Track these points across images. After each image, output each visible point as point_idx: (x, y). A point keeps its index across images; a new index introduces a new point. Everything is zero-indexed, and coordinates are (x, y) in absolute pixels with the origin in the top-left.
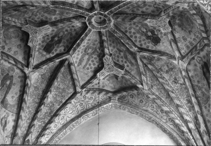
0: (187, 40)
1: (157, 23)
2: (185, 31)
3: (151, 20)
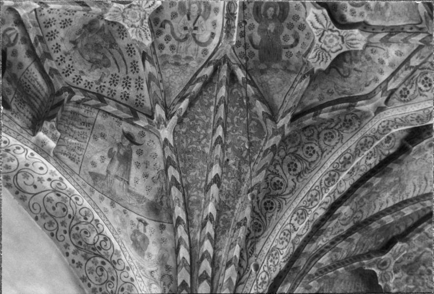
0: (61, 27)
1: (140, 9)
2: (80, 32)
3: (155, 5)
